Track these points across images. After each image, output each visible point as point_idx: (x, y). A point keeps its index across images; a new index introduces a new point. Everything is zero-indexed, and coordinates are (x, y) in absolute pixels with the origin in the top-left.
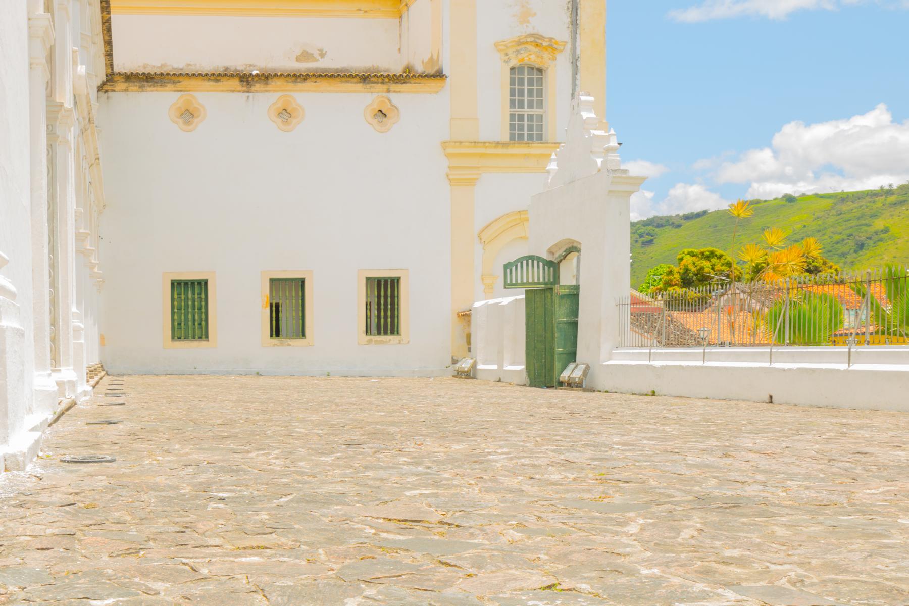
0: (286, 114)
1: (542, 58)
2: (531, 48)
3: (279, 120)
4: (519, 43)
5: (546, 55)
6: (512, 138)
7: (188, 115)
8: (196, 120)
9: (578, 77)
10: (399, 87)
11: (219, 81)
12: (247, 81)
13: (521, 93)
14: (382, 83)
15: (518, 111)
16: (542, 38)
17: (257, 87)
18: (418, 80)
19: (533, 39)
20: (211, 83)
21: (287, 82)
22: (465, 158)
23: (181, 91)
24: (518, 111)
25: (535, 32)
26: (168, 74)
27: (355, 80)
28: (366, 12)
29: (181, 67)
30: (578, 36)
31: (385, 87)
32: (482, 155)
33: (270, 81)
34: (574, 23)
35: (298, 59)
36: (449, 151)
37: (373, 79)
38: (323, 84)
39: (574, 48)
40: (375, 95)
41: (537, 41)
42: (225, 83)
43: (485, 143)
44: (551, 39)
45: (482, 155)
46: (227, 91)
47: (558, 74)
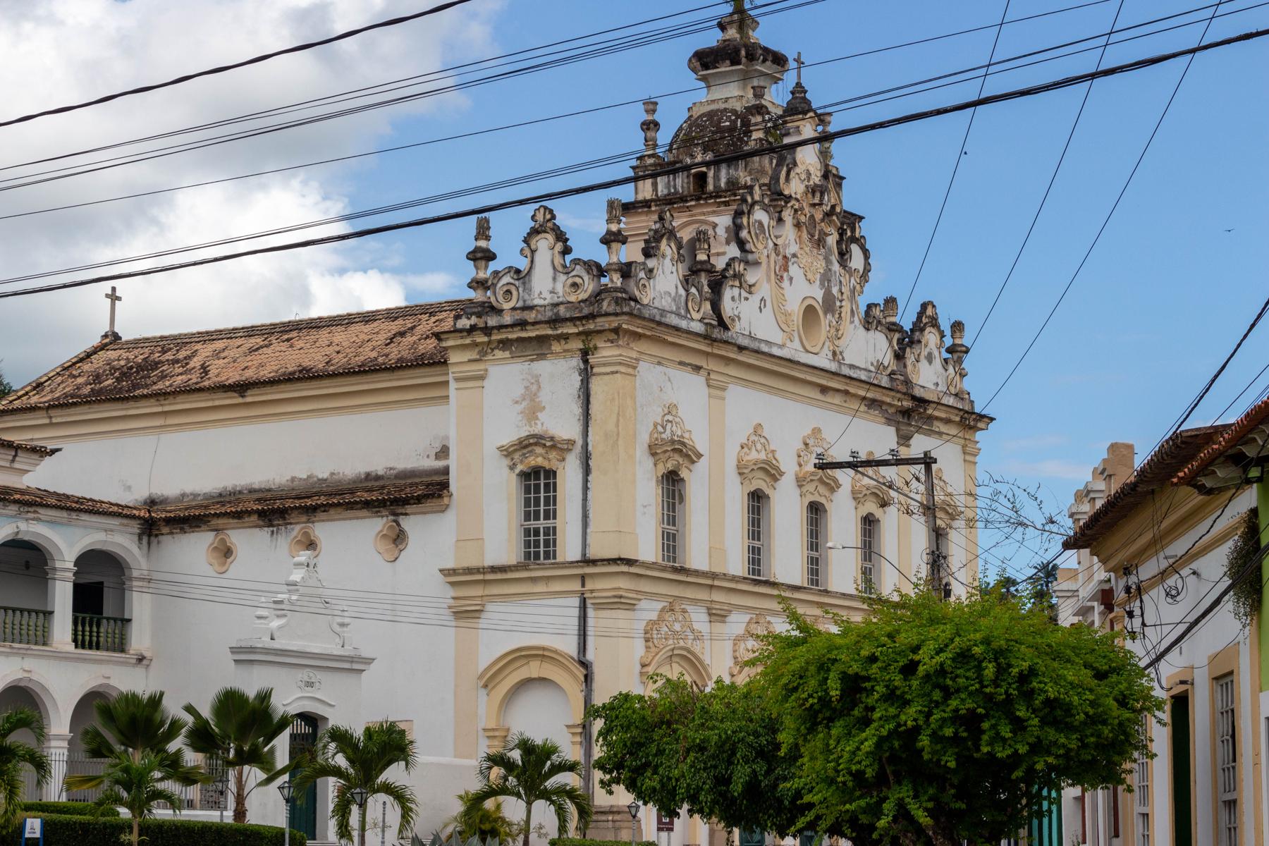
2: (539, 450)
5: (553, 455)
9: (590, 478)
13: (537, 503)
16: (541, 437)
24: (533, 524)
32: (485, 582)
39: (586, 445)
44: (552, 438)
45: (485, 582)
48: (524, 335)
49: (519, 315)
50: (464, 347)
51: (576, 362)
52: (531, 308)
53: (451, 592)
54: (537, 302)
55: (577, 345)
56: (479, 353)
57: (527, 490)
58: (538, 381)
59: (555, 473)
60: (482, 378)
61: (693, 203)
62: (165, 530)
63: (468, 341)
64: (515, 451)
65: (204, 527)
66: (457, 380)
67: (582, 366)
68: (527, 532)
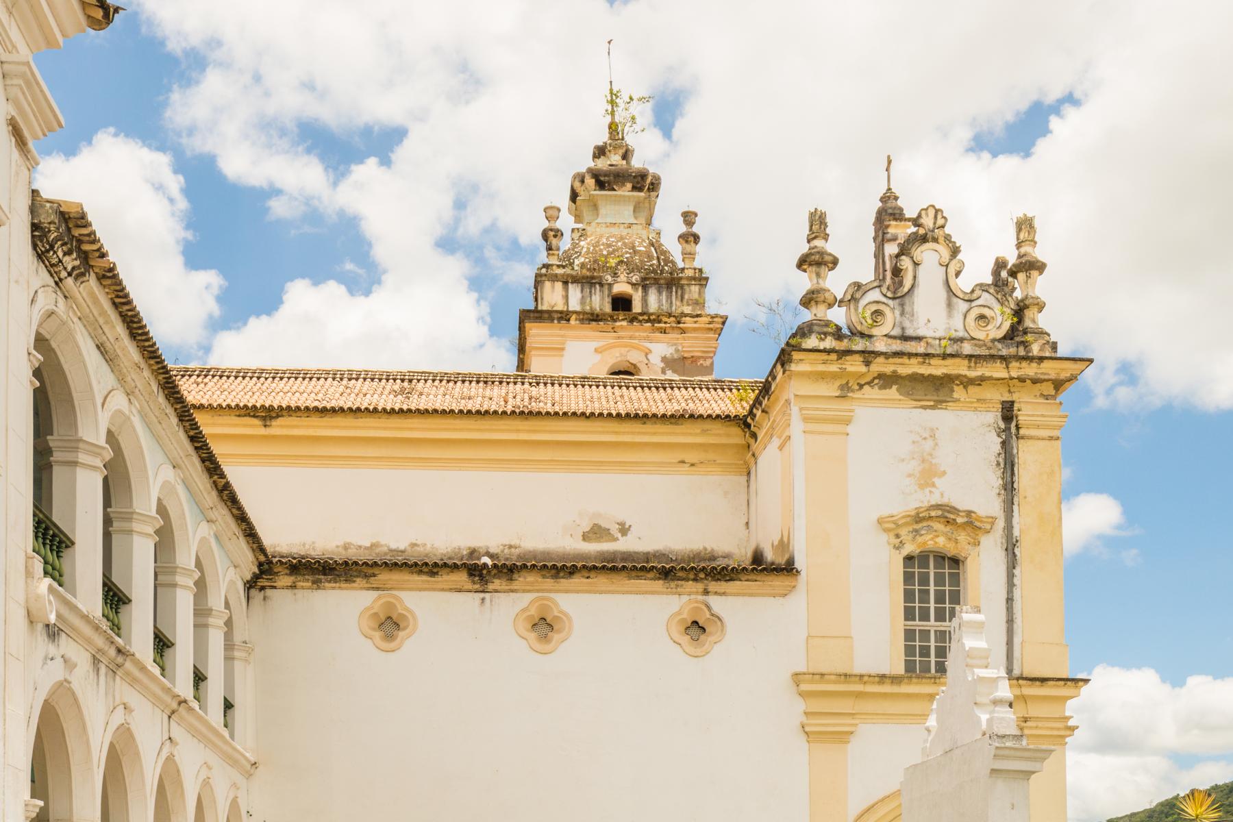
0: (544, 626)
1: (956, 541)
3: (532, 636)
4: (918, 519)
5: (963, 537)
6: (910, 667)
7: (390, 625)
8: (401, 634)
9: (1016, 572)
10: (722, 586)
11: (437, 573)
12: (481, 576)
14: (695, 580)
15: (917, 624)
16: (954, 510)
17: (497, 584)
18: (752, 577)
19: (940, 513)
20: (425, 578)
21: (544, 577)
22: (832, 699)
23: (378, 589)
25: (945, 501)
26: (356, 563)
27: (651, 575)
28: (692, 465)
29: (402, 547)
30: (1015, 508)
31: (700, 586)
32: (859, 695)
33: (515, 576)
34: (1009, 488)
35: (585, 537)
36: (804, 687)
37: (680, 574)
38: (601, 580)
39: (1009, 527)
40: (685, 598)
41: (946, 514)
42: (445, 577)
43: (861, 676)
45: (859, 695)
46: (450, 590)
47: (984, 568)
48: (925, 370)
49: (897, 346)
50: (822, 376)
51: (993, 417)
52: (919, 339)
53: (800, 706)
54: (921, 333)
55: (997, 395)
56: (842, 387)
57: (908, 578)
58: (933, 436)
59: (956, 562)
60: (847, 422)
61: (624, 323)
62: (285, 580)
63: (834, 368)
64: (906, 524)
65: (360, 582)
66: (806, 419)
67: (1002, 426)
68: (909, 634)
